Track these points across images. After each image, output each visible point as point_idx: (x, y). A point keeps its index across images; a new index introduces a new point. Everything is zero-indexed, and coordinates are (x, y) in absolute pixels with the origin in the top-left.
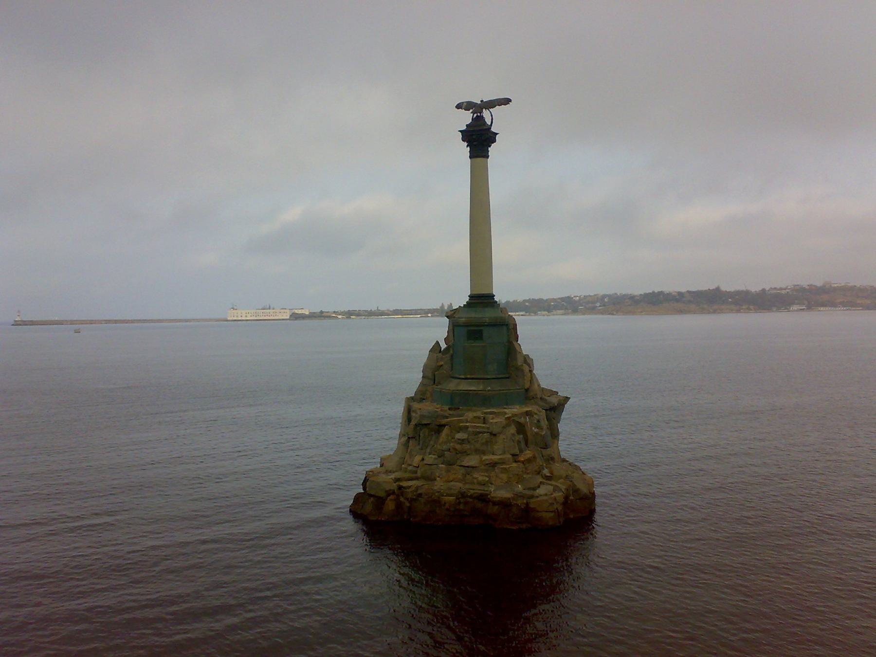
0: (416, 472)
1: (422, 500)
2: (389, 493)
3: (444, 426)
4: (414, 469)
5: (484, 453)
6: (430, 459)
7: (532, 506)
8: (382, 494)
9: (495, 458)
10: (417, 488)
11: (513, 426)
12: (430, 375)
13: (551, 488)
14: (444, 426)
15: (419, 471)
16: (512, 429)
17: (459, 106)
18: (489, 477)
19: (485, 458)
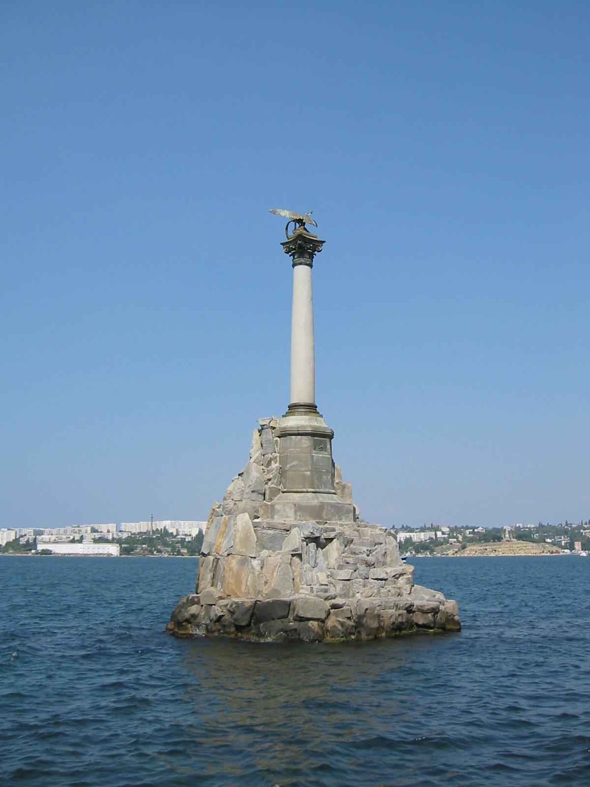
14: (331, 540)
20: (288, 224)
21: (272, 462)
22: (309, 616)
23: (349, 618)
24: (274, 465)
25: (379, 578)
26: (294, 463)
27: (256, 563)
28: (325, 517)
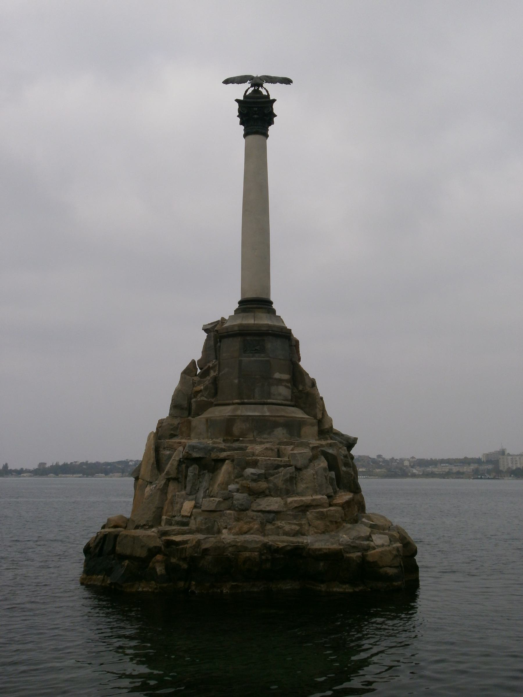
0: (186, 524)
1: (209, 558)
2: (153, 552)
3: (223, 460)
4: (185, 520)
6: (208, 504)
7: (370, 559)
8: (141, 553)
9: (307, 499)
10: (199, 542)
11: (323, 458)
12: (185, 404)
13: (387, 538)
14: (223, 460)
15: (192, 521)
16: (323, 463)
18: (300, 525)
19: (290, 500)
24: (212, 374)
25: (264, 509)
26: (226, 370)
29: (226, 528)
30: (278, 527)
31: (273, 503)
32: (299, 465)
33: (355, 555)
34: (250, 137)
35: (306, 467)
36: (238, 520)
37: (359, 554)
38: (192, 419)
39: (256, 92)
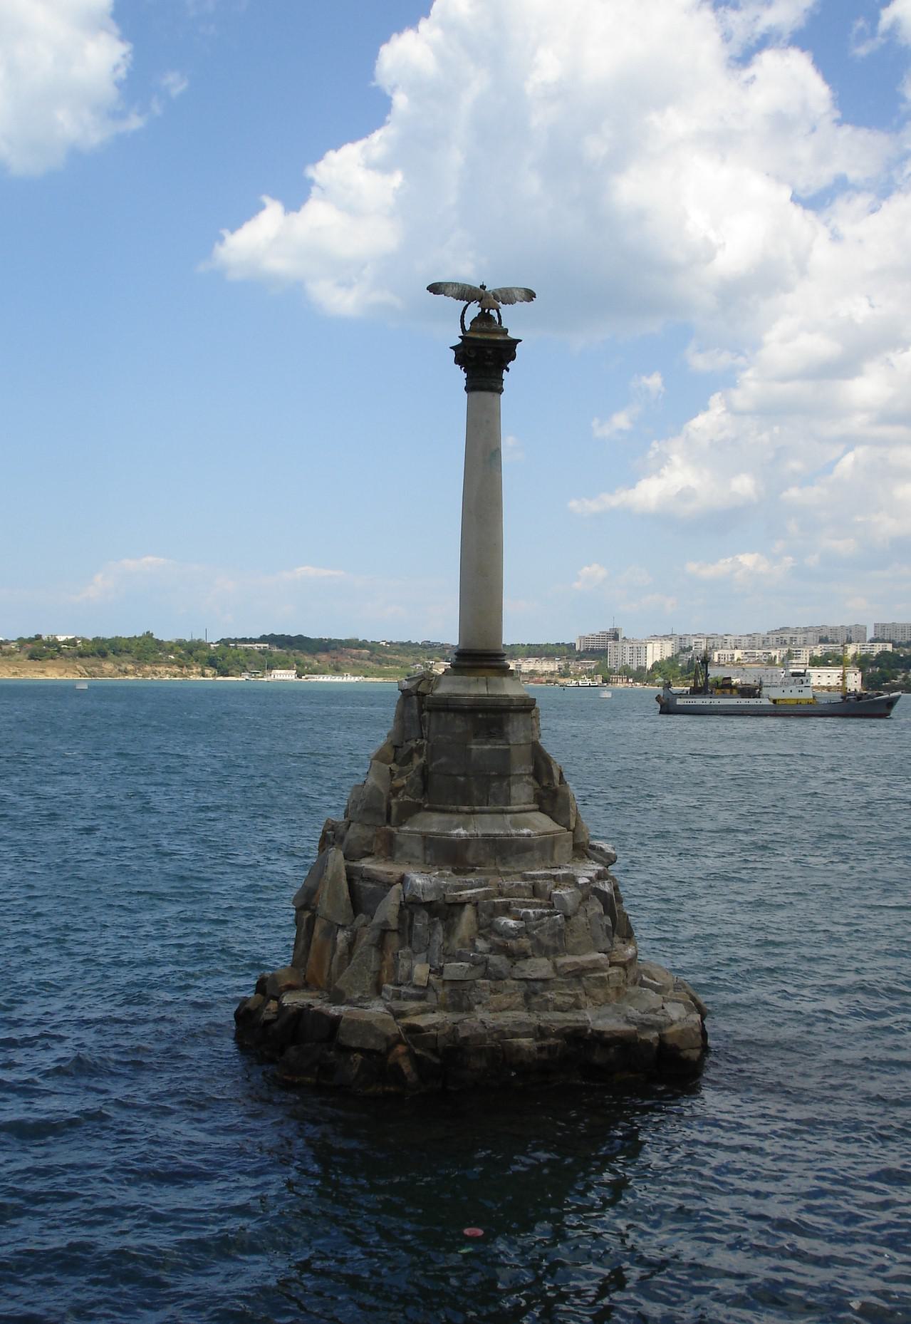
5: (556, 951)
7: (669, 1041)
8: (382, 1046)
15: (431, 995)
17: (435, 289)
19: (561, 961)
20: (464, 313)
21: (415, 755)
22: (354, 1044)
23: (434, 1051)
24: (418, 761)
26: (443, 760)
27: (342, 936)
28: (471, 861)
29: (479, 1003)
30: (548, 1000)
31: (539, 967)
32: (569, 912)
33: (652, 1035)
34: (475, 394)
35: (575, 914)
36: (494, 991)
37: (656, 1034)
38: (394, 830)
39: (484, 317)
